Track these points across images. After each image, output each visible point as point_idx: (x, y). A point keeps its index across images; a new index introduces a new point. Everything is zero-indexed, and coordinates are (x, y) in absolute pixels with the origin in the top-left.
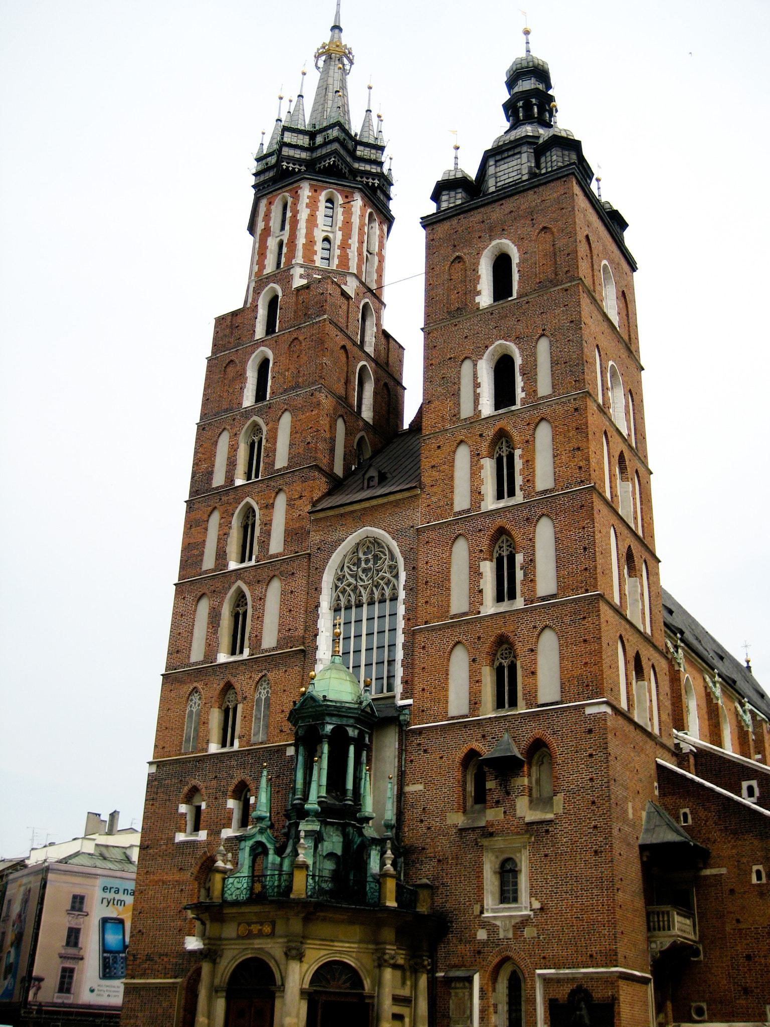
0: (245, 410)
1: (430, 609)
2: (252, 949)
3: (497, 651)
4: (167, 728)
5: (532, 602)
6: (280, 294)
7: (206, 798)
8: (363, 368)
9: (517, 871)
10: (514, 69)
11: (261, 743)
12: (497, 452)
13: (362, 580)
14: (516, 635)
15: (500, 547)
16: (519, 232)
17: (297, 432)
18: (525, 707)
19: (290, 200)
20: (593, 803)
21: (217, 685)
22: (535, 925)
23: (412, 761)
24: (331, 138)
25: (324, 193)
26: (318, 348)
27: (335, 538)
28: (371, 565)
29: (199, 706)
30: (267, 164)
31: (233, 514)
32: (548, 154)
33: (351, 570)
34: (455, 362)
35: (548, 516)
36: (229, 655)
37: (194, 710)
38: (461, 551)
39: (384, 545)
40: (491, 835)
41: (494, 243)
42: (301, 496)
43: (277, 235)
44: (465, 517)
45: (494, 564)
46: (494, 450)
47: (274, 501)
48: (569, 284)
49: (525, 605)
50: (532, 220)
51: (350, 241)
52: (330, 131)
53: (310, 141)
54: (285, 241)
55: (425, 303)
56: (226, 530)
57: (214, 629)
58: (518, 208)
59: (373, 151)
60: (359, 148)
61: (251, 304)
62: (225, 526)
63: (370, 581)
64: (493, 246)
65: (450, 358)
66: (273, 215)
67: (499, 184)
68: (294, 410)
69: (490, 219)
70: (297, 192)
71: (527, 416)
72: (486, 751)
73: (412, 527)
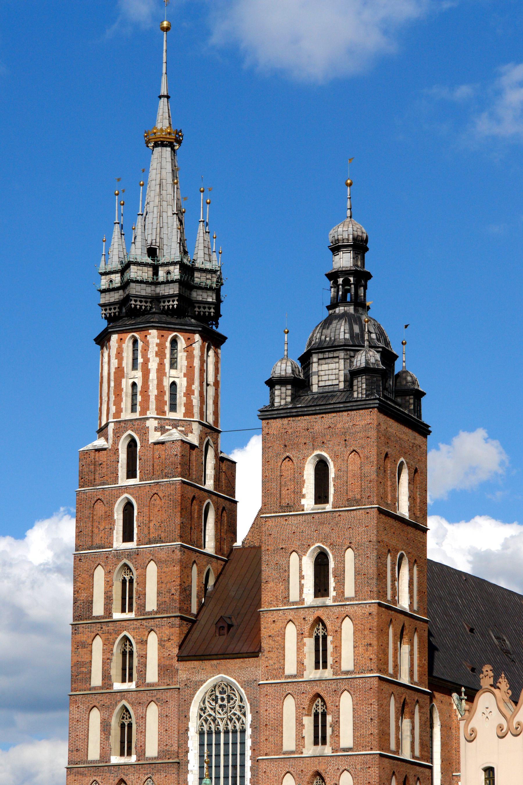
1: (269, 745)
3: (313, 780)
5: (337, 751)
10: (336, 238)
12: (316, 632)
13: (219, 713)
14: (326, 773)
15: (317, 706)
19: (140, 344)
27: (198, 678)
28: (225, 702)
32: (359, 379)
33: (210, 704)
34: (286, 553)
35: (348, 691)
36: (118, 757)
39: (235, 689)
45: (312, 718)
46: (313, 630)
47: (147, 638)
49: (332, 753)
50: (345, 440)
51: (194, 387)
52: (171, 268)
53: (153, 276)
54: (139, 388)
59: (209, 276)
60: (197, 274)
61: (112, 446)
62: (107, 652)
63: (225, 716)
65: (282, 548)
66: (125, 354)
67: (321, 384)
69: (313, 429)
70: (146, 336)
71: (336, 610)
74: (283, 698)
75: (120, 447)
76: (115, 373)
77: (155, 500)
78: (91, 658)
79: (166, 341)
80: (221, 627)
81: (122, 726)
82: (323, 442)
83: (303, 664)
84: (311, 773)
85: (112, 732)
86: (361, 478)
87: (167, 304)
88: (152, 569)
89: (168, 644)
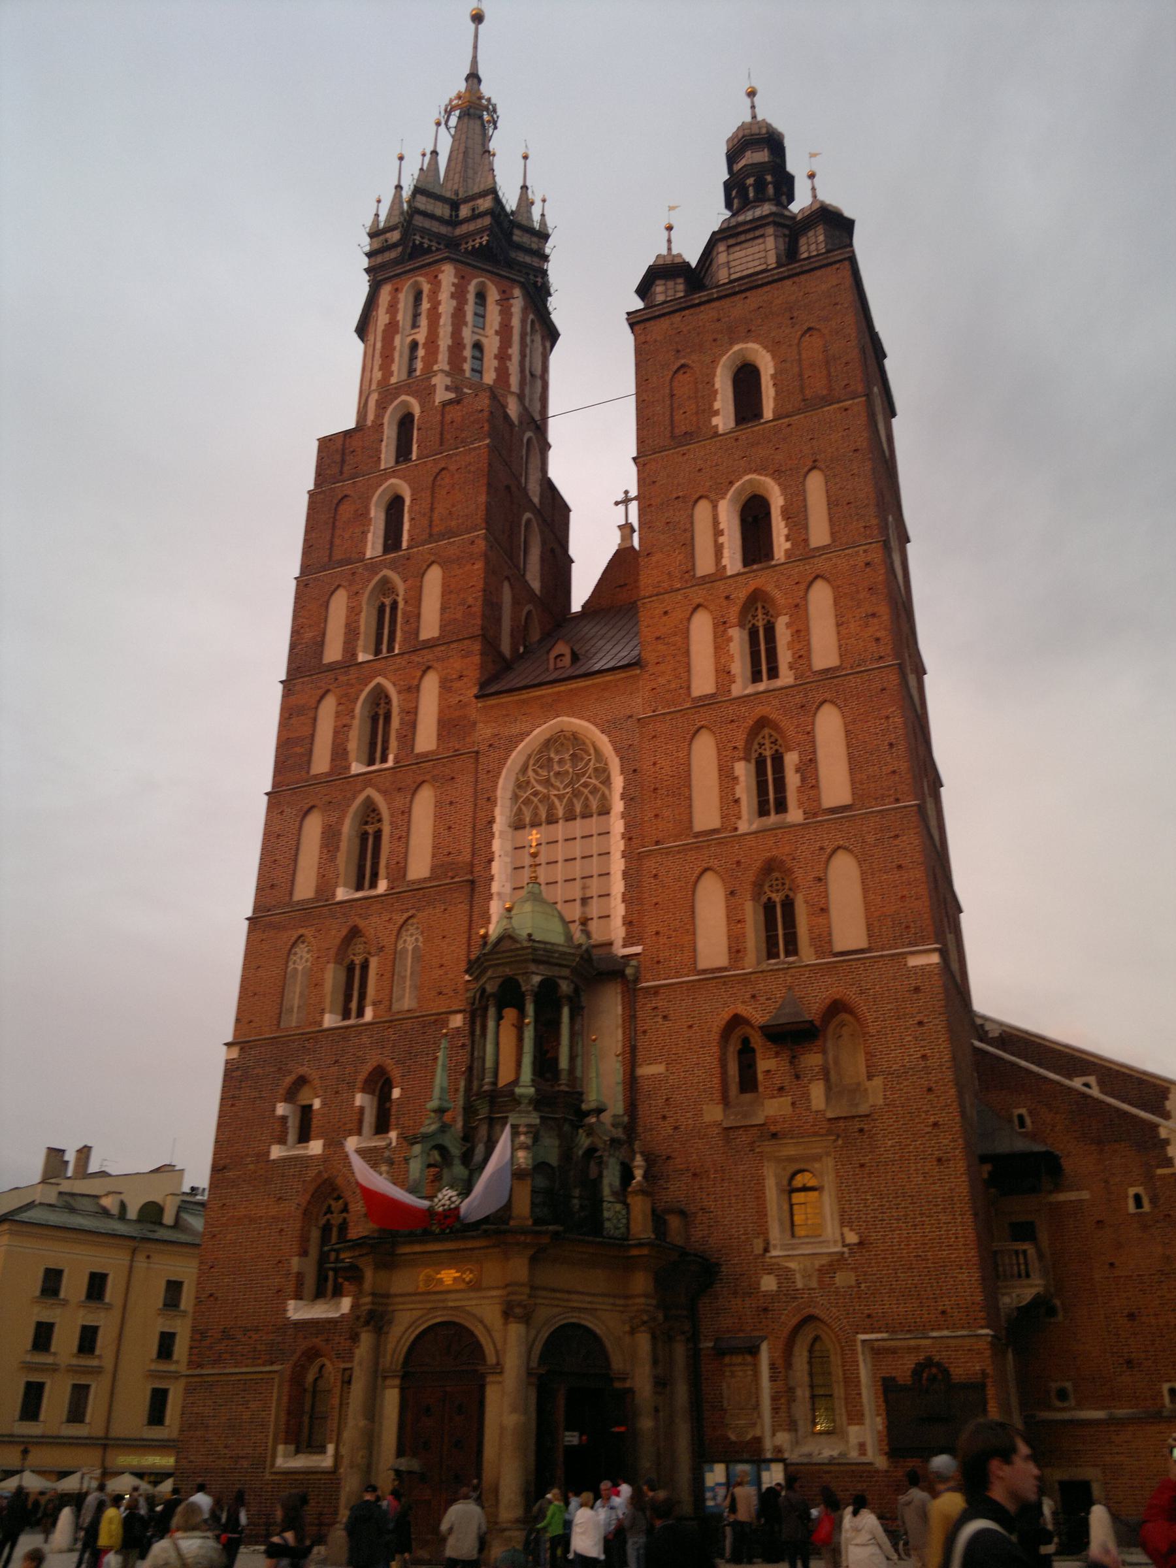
2: (445, 1308)
4: (255, 994)
5: (815, 815)
6: (417, 411)
7: (321, 1093)
8: (529, 521)
10: (740, 136)
11: (408, 1011)
14: (794, 859)
16: (772, 335)
17: (451, 592)
18: (814, 957)
19: (426, 288)
20: (930, 1090)
21: (337, 933)
22: (852, 1268)
23: (645, 1032)
24: (482, 209)
25: (474, 282)
27: (515, 729)
29: (307, 961)
30: (386, 241)
31: (357, 699)
32: (811, 233)
35: (832, 702)
36: (352, 891)
37: (300, 968)
39: (587, 741)
40: (774, 1136)
41: (736, 348)
43: (408, 333)
45: (752, 767)
48: (850, 402)
51: (510, 351)
52: (480, 201)
55: (637, 424)
56: (346, 720)
57: (331, 854)
58: (771, 303)
59: (535, 239)
61: (373, 421)
63: (569, 790)
64: (734, 353)
65: (678, 498)
66: (401, 306)
68: (445, 564)
69: (729, 317)
70: (436, 277)
72: (759, 1016)
73: (630, 717)
75: (386, 420)
76: (384, 331)
77: (442, 479)
78: (314, 731)
79: (469, 284)
80: (556, 657)
81: (364, 837)
82: (749, 331)
83: (729, 672)
84: (758, 864)
85: (344, 845)
86: (827, 363)
87: (471, 243)
88: (434, 578)
89: (457, 685)
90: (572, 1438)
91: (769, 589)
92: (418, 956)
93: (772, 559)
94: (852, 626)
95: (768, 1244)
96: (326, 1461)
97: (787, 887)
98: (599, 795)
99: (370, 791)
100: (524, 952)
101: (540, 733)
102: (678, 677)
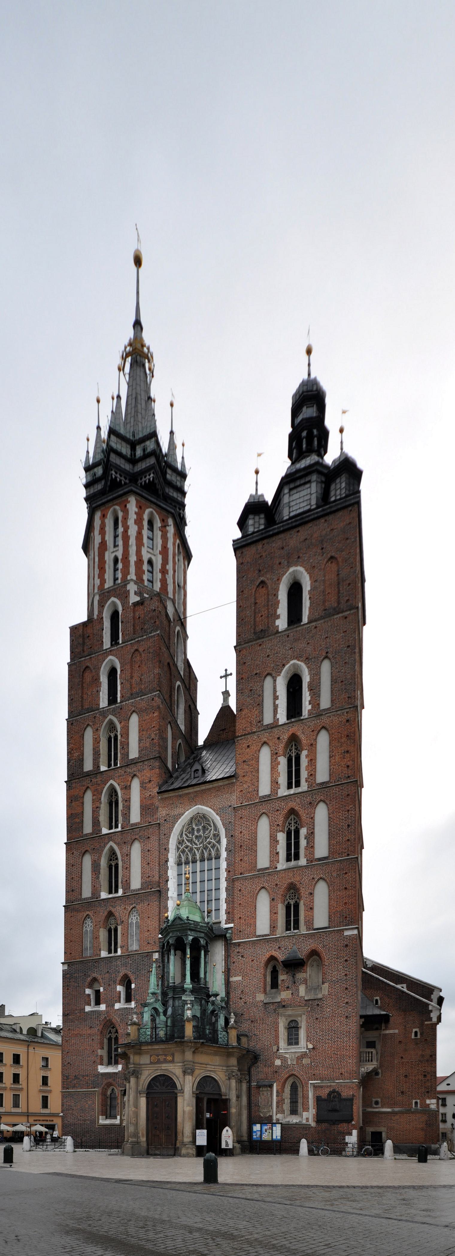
0: (102, 710)
1: (244, 864)
3: (287, 894)
9: (298, 1028)
12: (288, 753)
15: (290, 824)
26: (154, 659)
38: (264, 825)
40: (284, 1006)
42: (150, 781)
44: (266, 800)
73: (230, 806)
74: (257, 818)
90: (208, 1115)
91: (299, 734)
92: (138, 927)
93: (301, 715)
94: (337, 758)
95: (279, 1048)
96: (117, 1121)
97: (296, 897)
98: (215, 848)
99: (111, 843)
100: (186, 925)
101: (188, 814)
102: (253, 784)
